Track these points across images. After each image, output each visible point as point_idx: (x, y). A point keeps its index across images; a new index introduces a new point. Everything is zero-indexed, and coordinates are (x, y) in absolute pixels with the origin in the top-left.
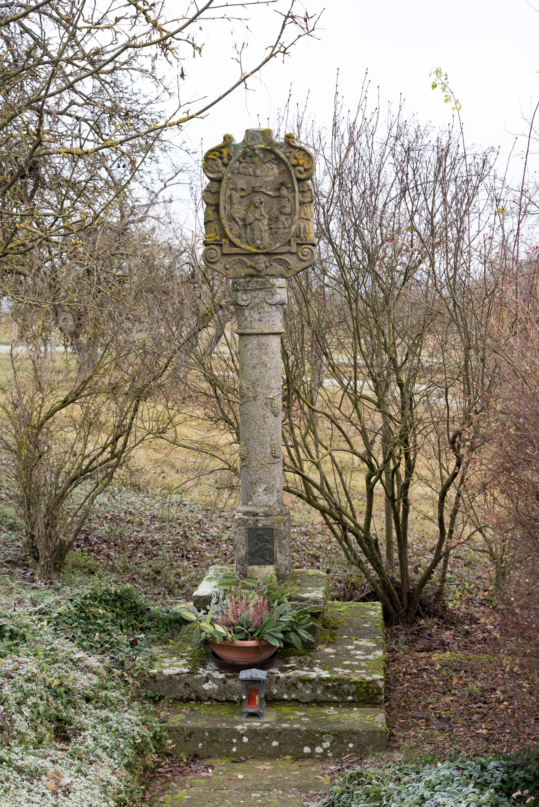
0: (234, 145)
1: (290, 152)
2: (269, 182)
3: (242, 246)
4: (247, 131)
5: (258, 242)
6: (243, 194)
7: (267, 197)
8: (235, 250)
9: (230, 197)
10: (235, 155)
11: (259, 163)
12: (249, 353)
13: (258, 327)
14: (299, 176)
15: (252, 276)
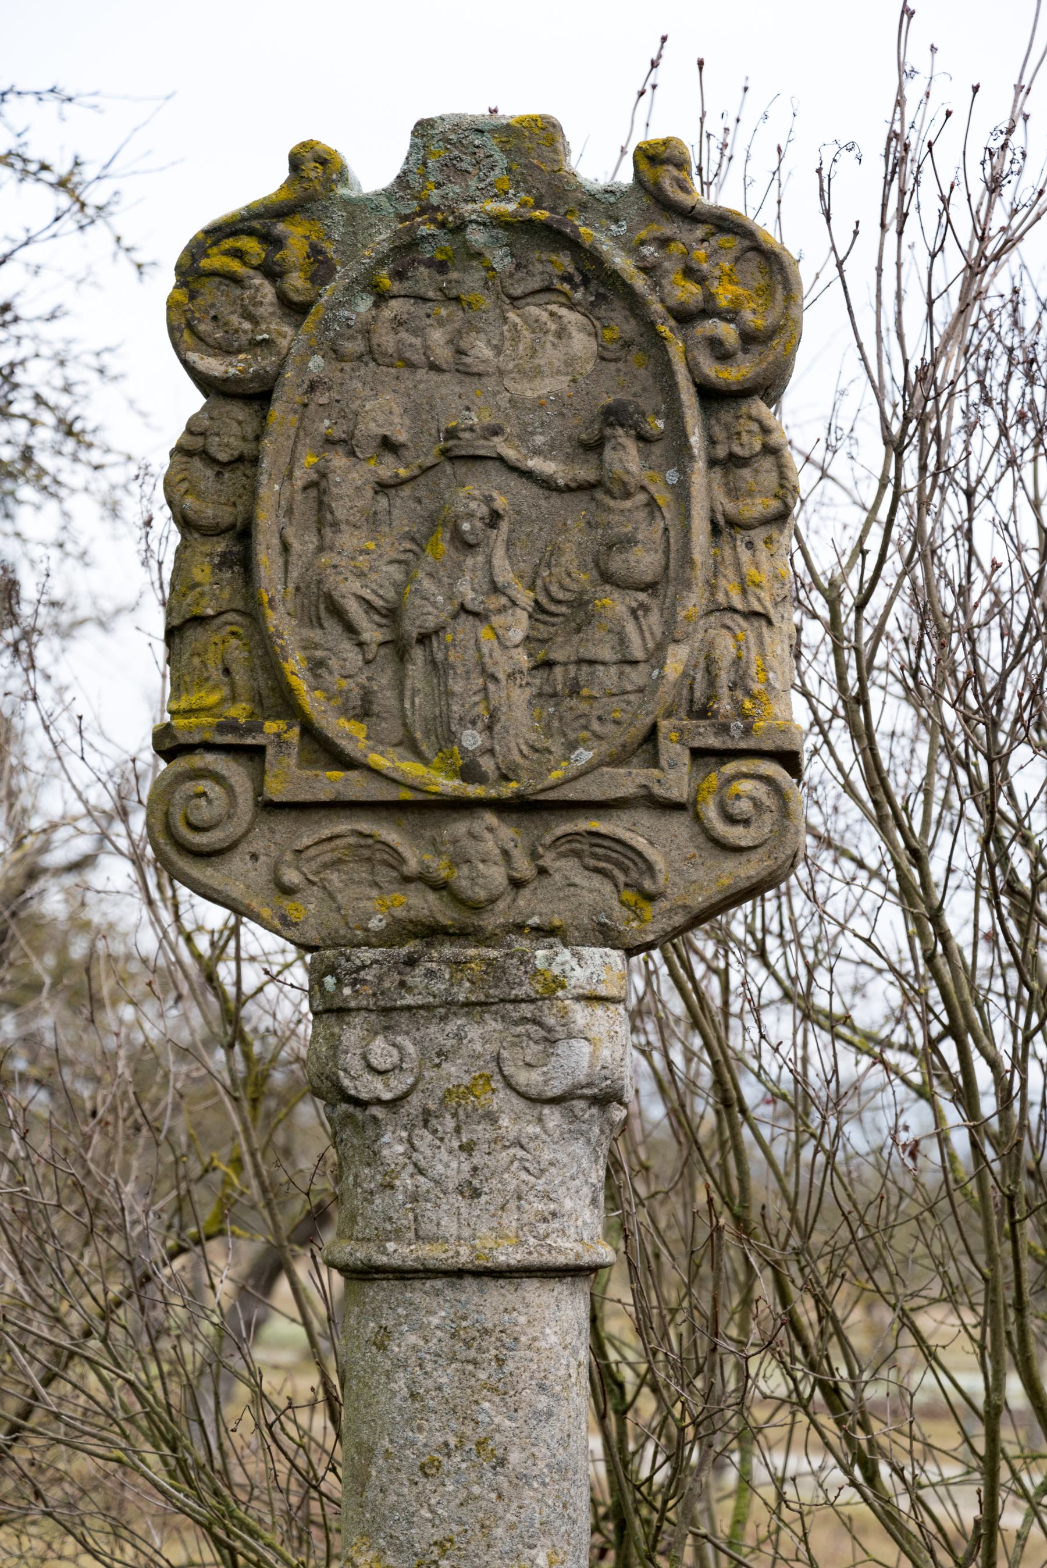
0: (348, 203)
1: (664, 243)
2: (539, 405)
3: (376, 759)
4: (423, 129)
5: (472, 739)
6: (388, 468)
7: (527, 491)
8: (331, 783)
9: (318, 485)
10: (350, 253)
11: (487, 302)
12: (400, 1384)
13: (460, 1233)
14: (712, 370)
15: (431, 933)
